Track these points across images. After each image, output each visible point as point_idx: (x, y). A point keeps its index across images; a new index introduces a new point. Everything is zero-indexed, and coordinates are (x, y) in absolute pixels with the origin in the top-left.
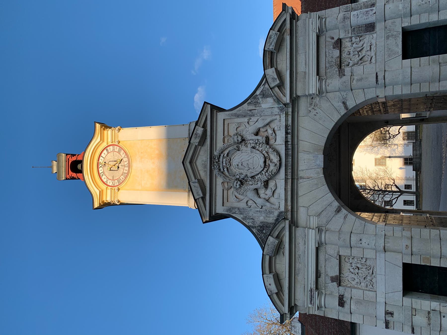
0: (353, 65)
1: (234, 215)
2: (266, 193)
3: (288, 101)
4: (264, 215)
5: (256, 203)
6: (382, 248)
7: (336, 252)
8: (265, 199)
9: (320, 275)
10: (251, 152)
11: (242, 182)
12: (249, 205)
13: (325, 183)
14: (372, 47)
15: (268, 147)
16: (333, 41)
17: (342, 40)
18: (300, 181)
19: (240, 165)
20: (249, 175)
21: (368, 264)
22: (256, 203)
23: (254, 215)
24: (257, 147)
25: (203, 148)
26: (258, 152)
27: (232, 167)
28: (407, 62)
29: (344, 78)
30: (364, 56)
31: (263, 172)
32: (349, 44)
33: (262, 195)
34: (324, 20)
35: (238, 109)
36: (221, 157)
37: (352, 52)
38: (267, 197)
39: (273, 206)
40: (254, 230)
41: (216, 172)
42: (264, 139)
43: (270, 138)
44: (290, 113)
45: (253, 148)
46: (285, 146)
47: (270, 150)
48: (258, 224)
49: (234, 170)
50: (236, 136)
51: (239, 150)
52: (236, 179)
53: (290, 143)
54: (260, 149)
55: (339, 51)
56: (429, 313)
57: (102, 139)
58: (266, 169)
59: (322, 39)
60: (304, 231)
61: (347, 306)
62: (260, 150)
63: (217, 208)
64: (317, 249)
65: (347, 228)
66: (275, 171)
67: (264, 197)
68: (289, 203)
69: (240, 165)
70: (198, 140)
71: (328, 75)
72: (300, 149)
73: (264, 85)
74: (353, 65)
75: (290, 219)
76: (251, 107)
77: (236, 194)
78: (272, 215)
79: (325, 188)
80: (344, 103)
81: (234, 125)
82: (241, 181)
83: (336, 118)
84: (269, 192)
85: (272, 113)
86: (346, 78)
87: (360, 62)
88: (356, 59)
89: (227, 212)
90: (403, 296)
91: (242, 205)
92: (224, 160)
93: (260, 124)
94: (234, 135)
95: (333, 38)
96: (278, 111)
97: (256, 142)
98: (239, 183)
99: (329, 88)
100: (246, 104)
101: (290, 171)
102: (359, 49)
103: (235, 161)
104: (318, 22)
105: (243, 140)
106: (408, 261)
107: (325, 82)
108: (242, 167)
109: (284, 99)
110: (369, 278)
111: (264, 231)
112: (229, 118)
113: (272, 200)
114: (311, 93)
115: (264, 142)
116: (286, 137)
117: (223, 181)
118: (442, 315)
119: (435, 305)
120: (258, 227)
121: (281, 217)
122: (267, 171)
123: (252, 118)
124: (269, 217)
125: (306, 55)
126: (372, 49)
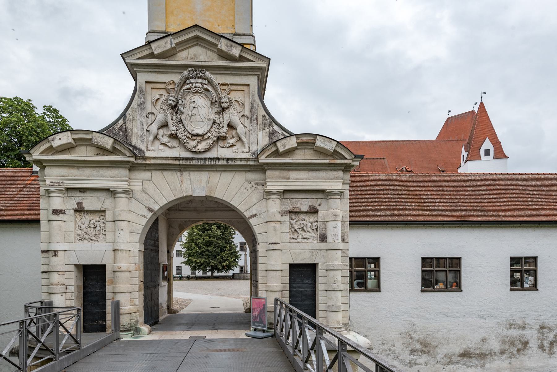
0: (291, 224)
1: (136, 96)
2: (165, 136)
3: (260, 161)
4: (139, 133)
5: (152, 124)
6: (117, 248)
7: (108, 208)
8: (158, 134)
9: (82, 192)
10: (209, 120)
11: (174, 107)
12: (150, 116)
13: (177, 197)
14: (305, 240)
15: (215, 139)
16: (317, 206)
17: (315, 215)
18: (179, 174)
19: (194, 105)
20: (183, 117)
21: (100, 236)
22: (152, 124)
23: (139, 122)
24: (215, 126)
25: (215, 56)
26: (209, 128)
27: (191, 95)
28: (287, 267)
29: (280, 215)
30: (298, 233)
31: (186, 133)
32: (312, 220)
33: (161, 132)
34: (339, 197)
35: (260, 103)
36: (203, 81)
37: (303, 222)
38: (160, 137)
39: (150, 143)
40: (121, 122)
42: (224, 134)
43: (225, 141)
44: (249, 163)
45: (214, 123)
46: (214, 158)
47: (210, 141)
48: (129, 125)
49: (188, 98)
50: (227, 101)
51: (212, 103)
52: (177, 100)
53: (217, 163)
54: (213, 130)
55: (306, 210)
56: (64, 284)
58: (190, 136)
59: (320, 196)
60: (126, 177)
61: (54, 217)
62: (212, 130)
63: (143, 74)
64: (107, 190)
66: (189, 146)
67: (159, 133)
68: (153, 162)
69: (194, 105)
71: (285, 200)
72: (213, 174)
73: (283, 135)
74: (291, 224)
75: (136, 162)
76: (260, 119)
77: (162, 100)
78: (140, 142)
79: (172, 198)
80: (255, 215)
81: (242, 98)
82: (176, 106)
83: (241, 208)
84: (165, 140)
85: (252, 143)
86: (279, 217)
87: (293, 229)
88: (296, 227)
89: (140, 88)
90: (75, 265)
91: (149, 107)
92: (200, 85)
93: (240, 129)
94: (229, 98)
95: (319, 205)
96: (253, 151)
97: (221, 125)
98: (174, 104)
99: (270, 201)
100: (265, 113)
101: (188, 162)
102: (305, 228)
103: (199, 99)
104: (337, 192)
105: (223, 110)
106: (108, 268)
107: (277, 198)
108: (191, 108)
109: (263, 157)
110: (87, 236)
111: (121, 133)
112: (250, 92)
113: (157, 143)
114: (268, 184)
115: (220, 134)
116: (223, 159)
117: (175, 82)
118: (64, 294)
119: (72, 289)
120: (125, 126)
121: (136, 152)
122: (188, 137)
123: (248, 121)
124: (137, 139)
125: (306, 179)
126: (303, 240)
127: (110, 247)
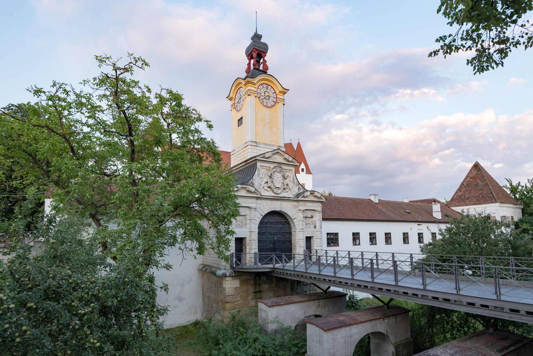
20: (273, 181)
41: (275, 165)
57: (280, 92)
64: (249, 207)
65: (256, 218)
70: (287, 158)
84: (266, 188)
91: (261, 176)
93: (290, 186)
106: (247, 239)
127: (248, 230)
